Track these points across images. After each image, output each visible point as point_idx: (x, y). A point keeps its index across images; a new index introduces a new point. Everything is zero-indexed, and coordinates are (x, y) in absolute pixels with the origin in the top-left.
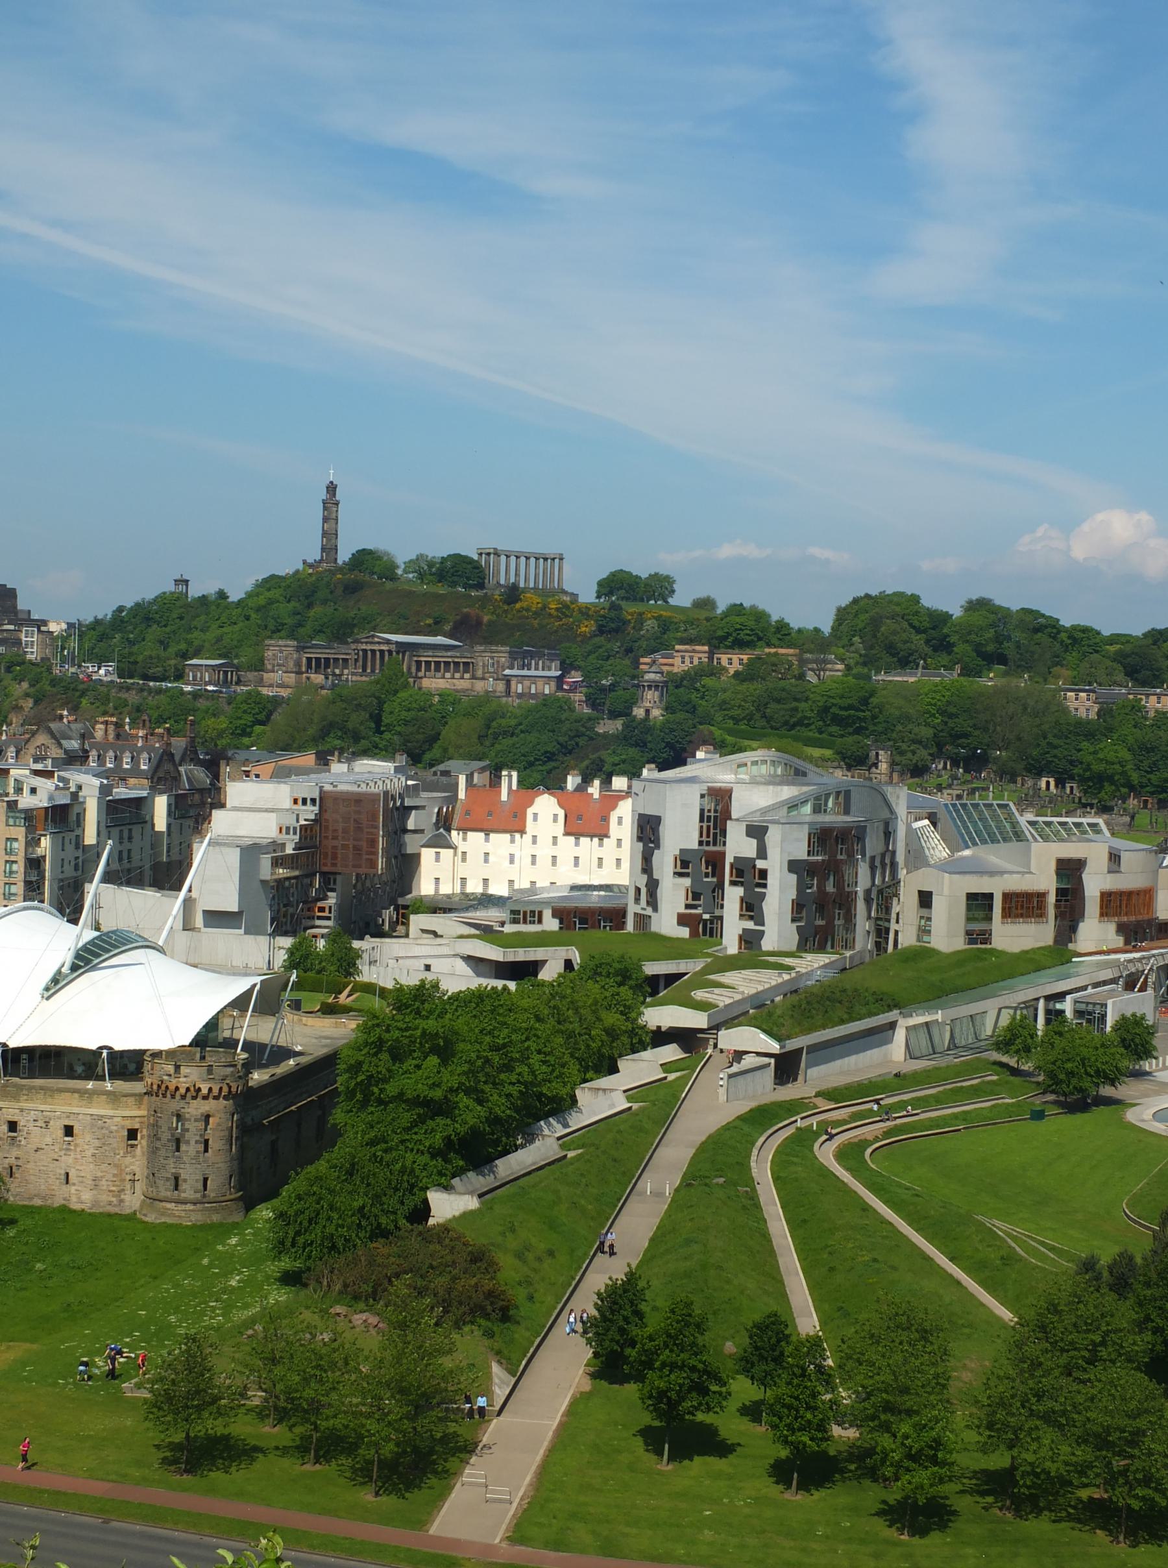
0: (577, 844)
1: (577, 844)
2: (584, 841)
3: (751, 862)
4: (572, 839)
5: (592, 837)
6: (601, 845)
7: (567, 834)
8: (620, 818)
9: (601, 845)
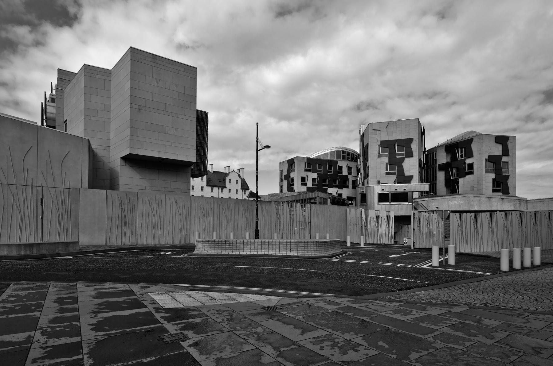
0: (212, 191)
1: (212, 191)
2: (216, 189)
3: (500, 158)
4: (210, 188)
5: (219, 187)
6: (222, 191)
7: (208, 185)
8: (230, 180)
9: (222, 191)
